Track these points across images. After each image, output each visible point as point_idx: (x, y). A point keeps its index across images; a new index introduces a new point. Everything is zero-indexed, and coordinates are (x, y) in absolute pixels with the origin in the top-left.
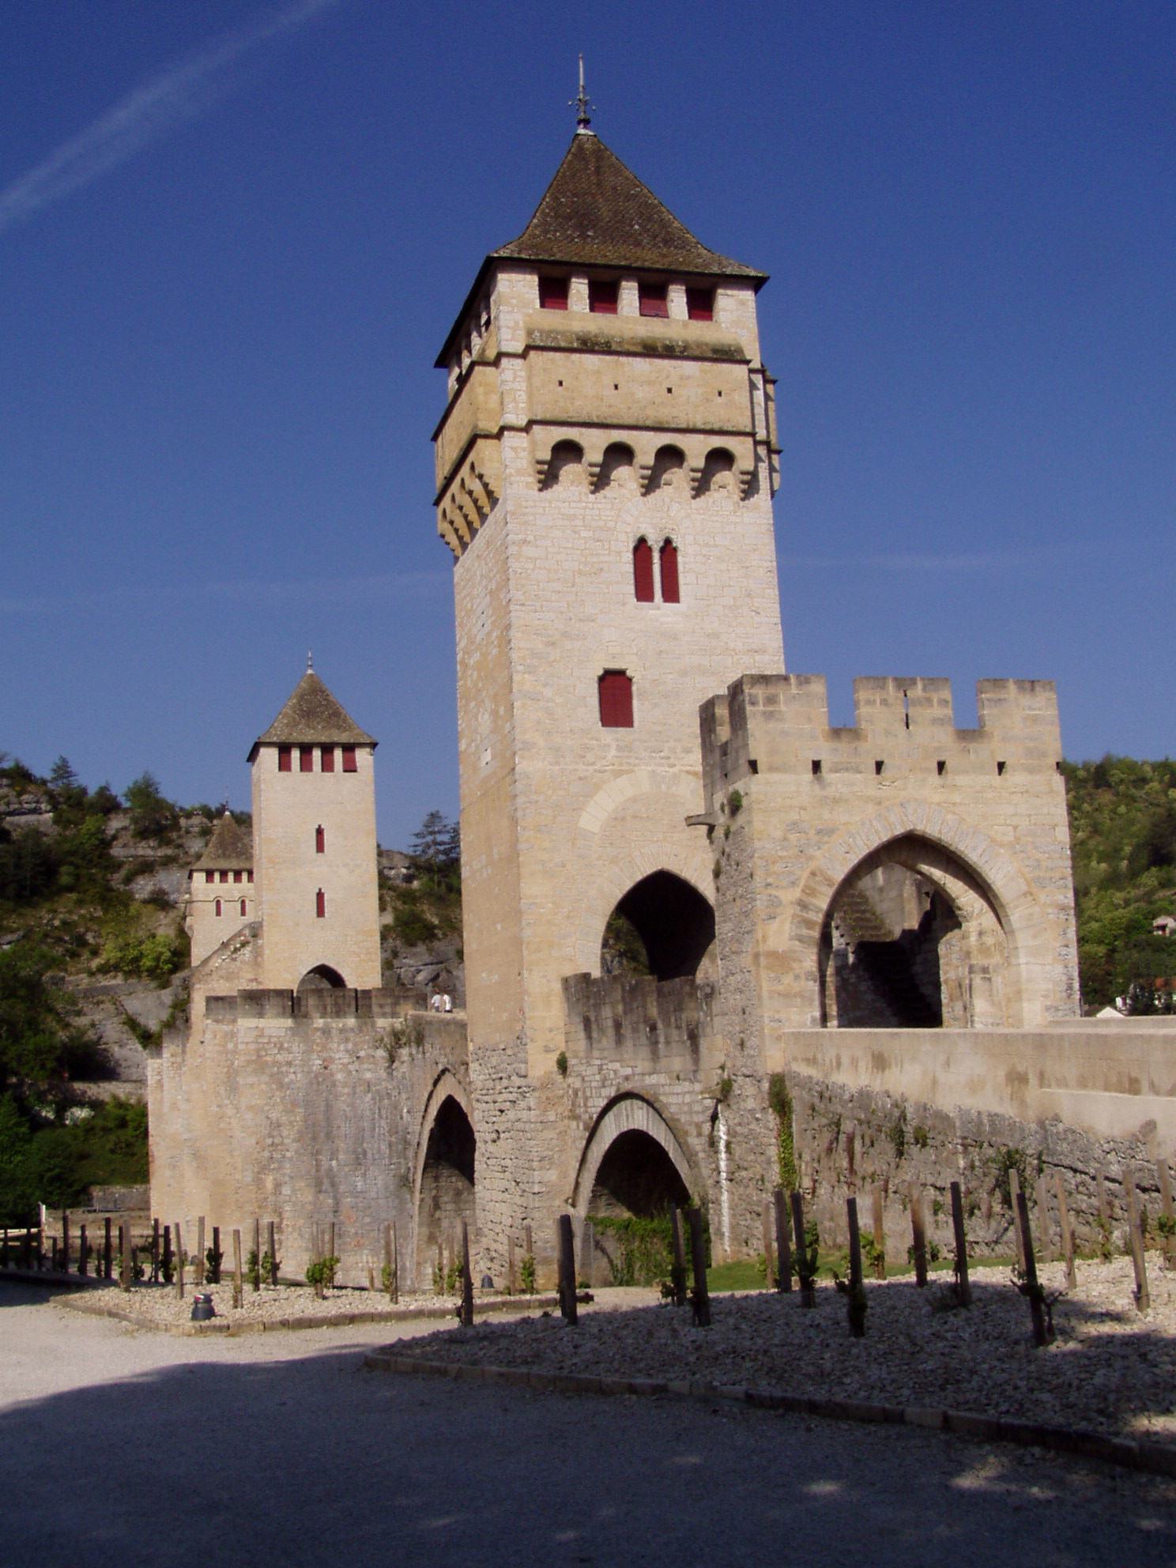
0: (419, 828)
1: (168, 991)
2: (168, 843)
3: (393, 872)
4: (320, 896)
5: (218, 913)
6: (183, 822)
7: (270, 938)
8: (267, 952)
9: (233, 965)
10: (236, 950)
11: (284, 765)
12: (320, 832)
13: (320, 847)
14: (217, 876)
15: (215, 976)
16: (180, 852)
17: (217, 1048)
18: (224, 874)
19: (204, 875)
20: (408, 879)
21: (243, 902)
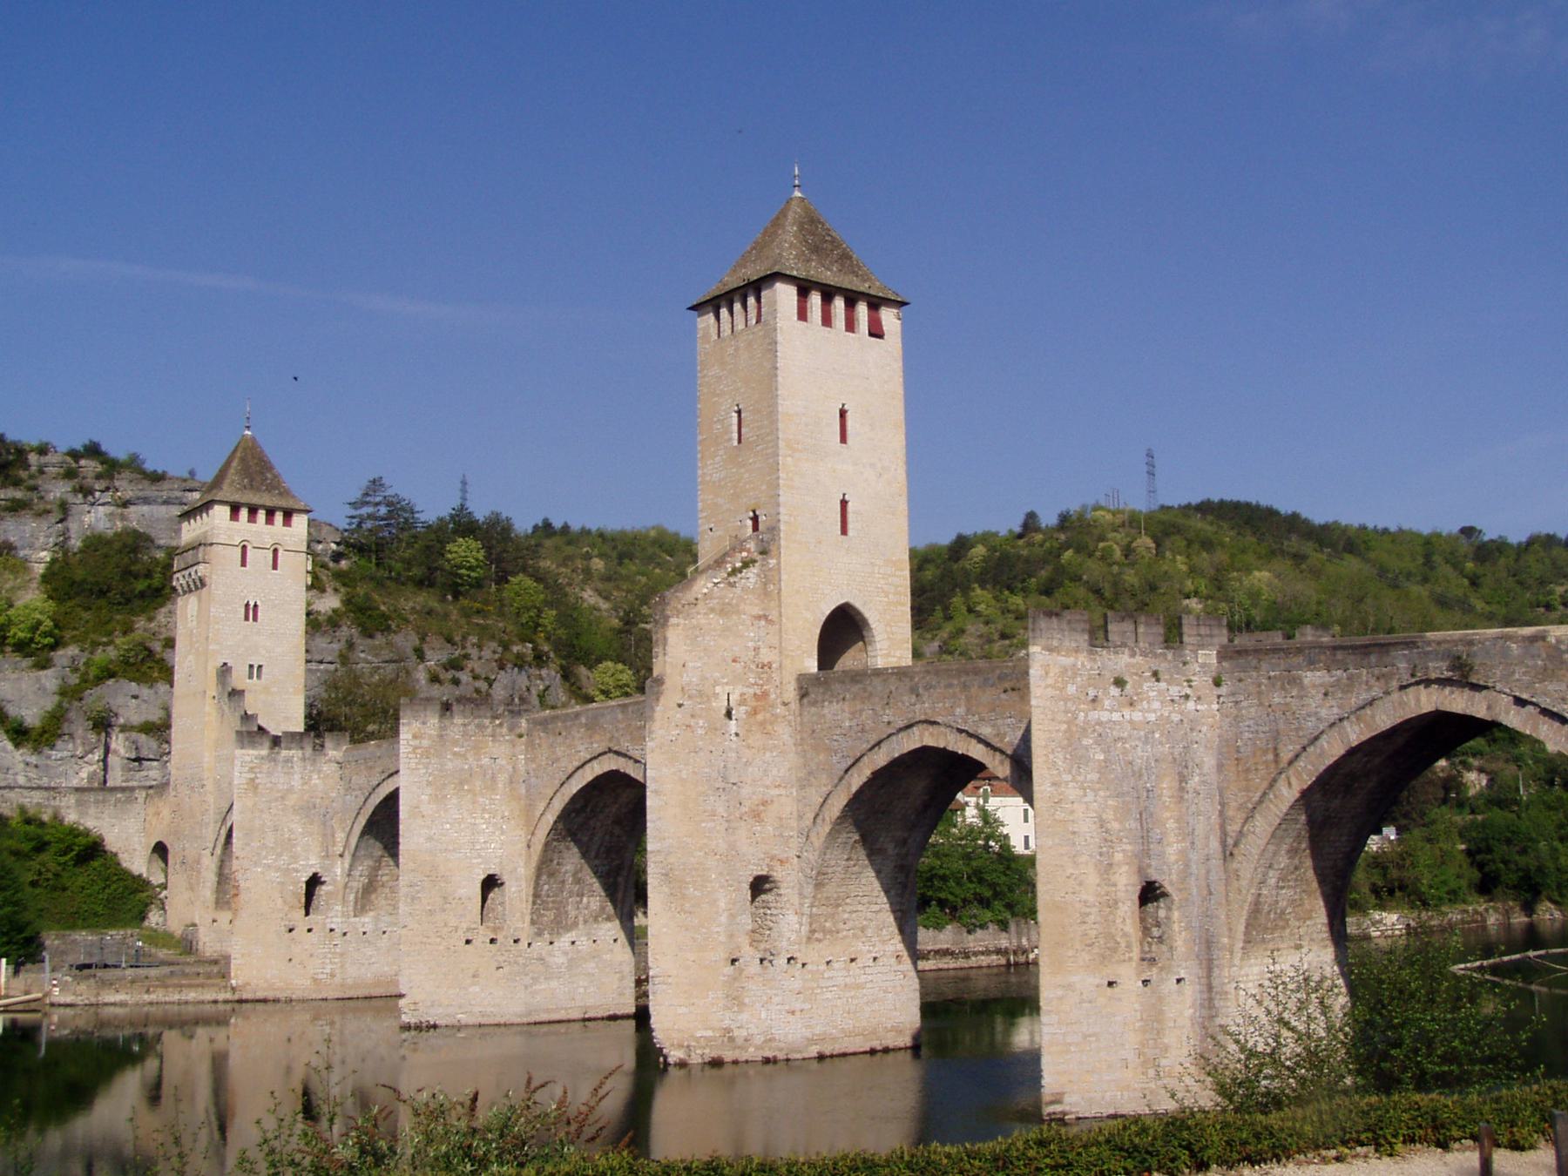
0: (356, 495)
1: (49, 672)
2: (17, 483)
3: (320, 547)
4: (844, 503)
5: (244, 564)
6: (33, 458)
7: (791, 556)
8: (784, 577)
9: (729, 594)
10: (735, 571)
11: (802, 315)
12: (843, 413)
13: (843, 439)
14: (244, 513)
15: (701, 607)
16: (34, 495)
17: (1050, 692)
18: (253, 511)
19: (226, 510)
20: (337, 557)
21: (275, 551)
